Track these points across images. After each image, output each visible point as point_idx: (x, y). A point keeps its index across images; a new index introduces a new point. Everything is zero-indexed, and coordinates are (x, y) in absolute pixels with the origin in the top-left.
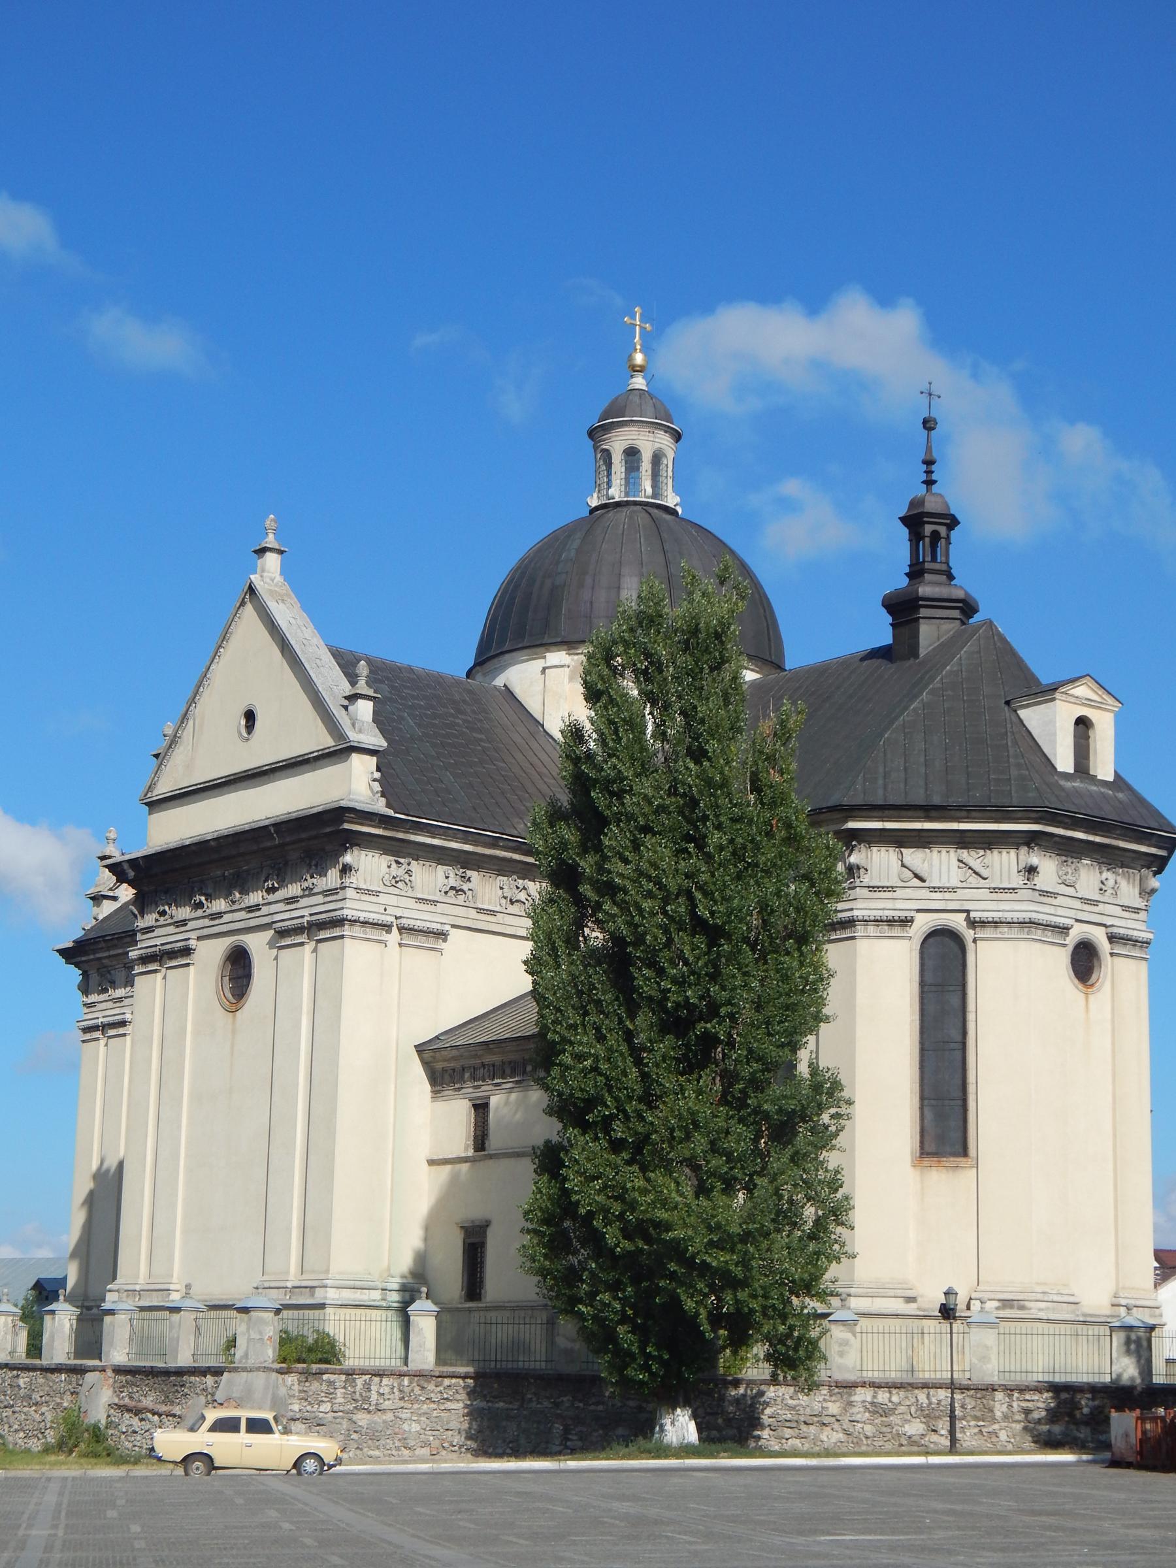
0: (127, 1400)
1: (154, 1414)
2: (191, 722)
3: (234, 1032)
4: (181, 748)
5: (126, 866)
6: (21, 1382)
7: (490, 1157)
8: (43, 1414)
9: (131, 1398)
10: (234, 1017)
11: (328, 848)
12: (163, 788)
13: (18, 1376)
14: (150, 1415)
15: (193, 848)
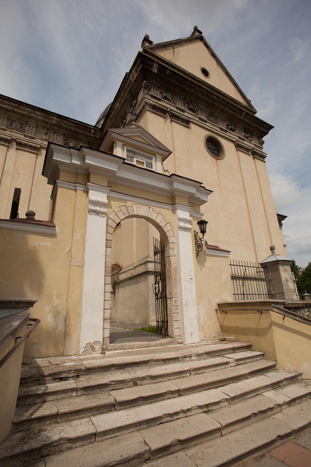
3: (218, 166)
5: (155, 65)
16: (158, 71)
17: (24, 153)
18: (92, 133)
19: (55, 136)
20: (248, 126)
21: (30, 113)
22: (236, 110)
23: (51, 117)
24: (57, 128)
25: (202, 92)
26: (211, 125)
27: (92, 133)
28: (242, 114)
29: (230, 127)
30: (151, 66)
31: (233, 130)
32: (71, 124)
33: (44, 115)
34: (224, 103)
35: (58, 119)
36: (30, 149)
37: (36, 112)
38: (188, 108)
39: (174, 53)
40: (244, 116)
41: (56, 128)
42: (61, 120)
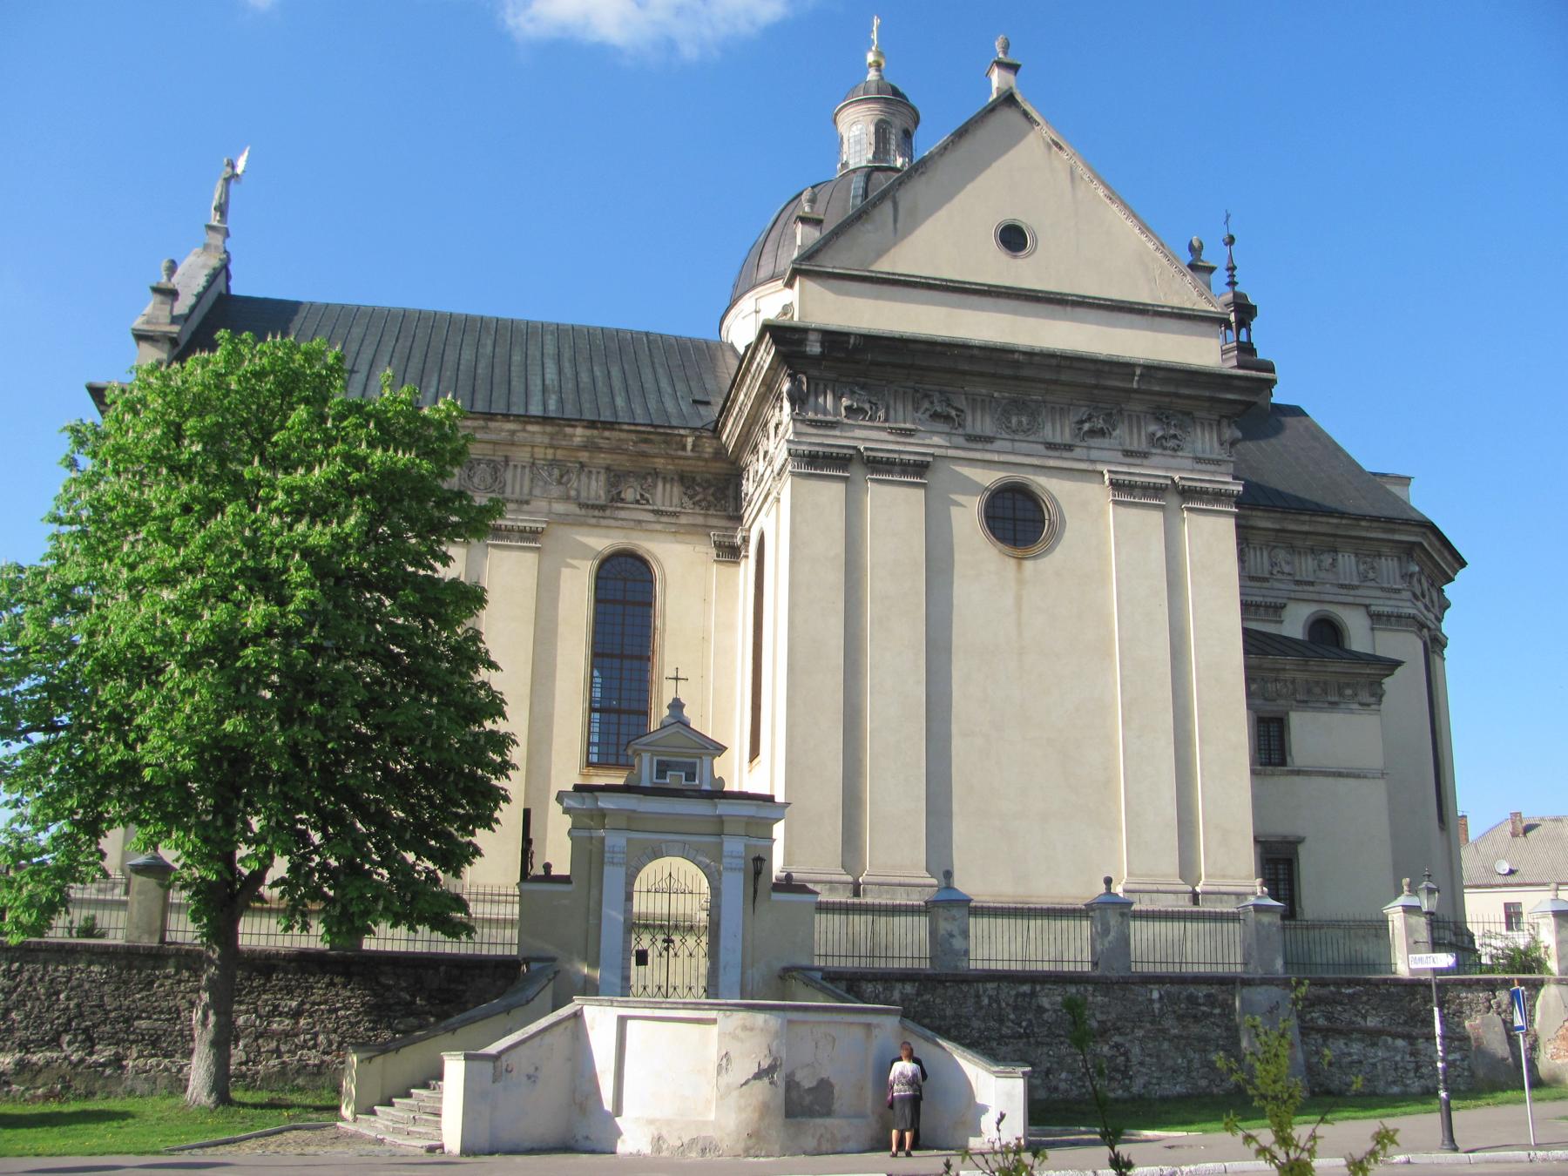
0: (1321, 1022)
1: (1395, 1036)
2: (887, 207)
3: (1021, 582)
4: (869, 227)
5: (812, 337)
6: (1045, 1002)
7: (1298, 772)
8: (1117, 1046)
9: (1328, 1019)
10: (1019, 566)
11: (1197, 414)
12: (828, 263)
13: (1033, 994)
14: (1390, 1040)
15: (976, 352)
16: (822, 345)
17: (505, 554)
18: (689, 447)
19: (584, 478)
20: (1167, 400)
21: (513, 433)
22: (1107, 368)
23: (568, 430)
24: (586, 454)
25: (972, 356)
26: (1008, 445)
27: (689, 447)
28: (1134, 374)
29: (1086, 426)
30: (802, 342)
31: (1101, 433)
32: (624, 436)
33: (549, 429)
34: (1054, 362)
35: (588, 432)
36: (522, 539)
37: (530, 428)
38: (927, 415)
39: (895, 221)
40: (1141, 375)
41: (584, 456)
42: (595, 432)
